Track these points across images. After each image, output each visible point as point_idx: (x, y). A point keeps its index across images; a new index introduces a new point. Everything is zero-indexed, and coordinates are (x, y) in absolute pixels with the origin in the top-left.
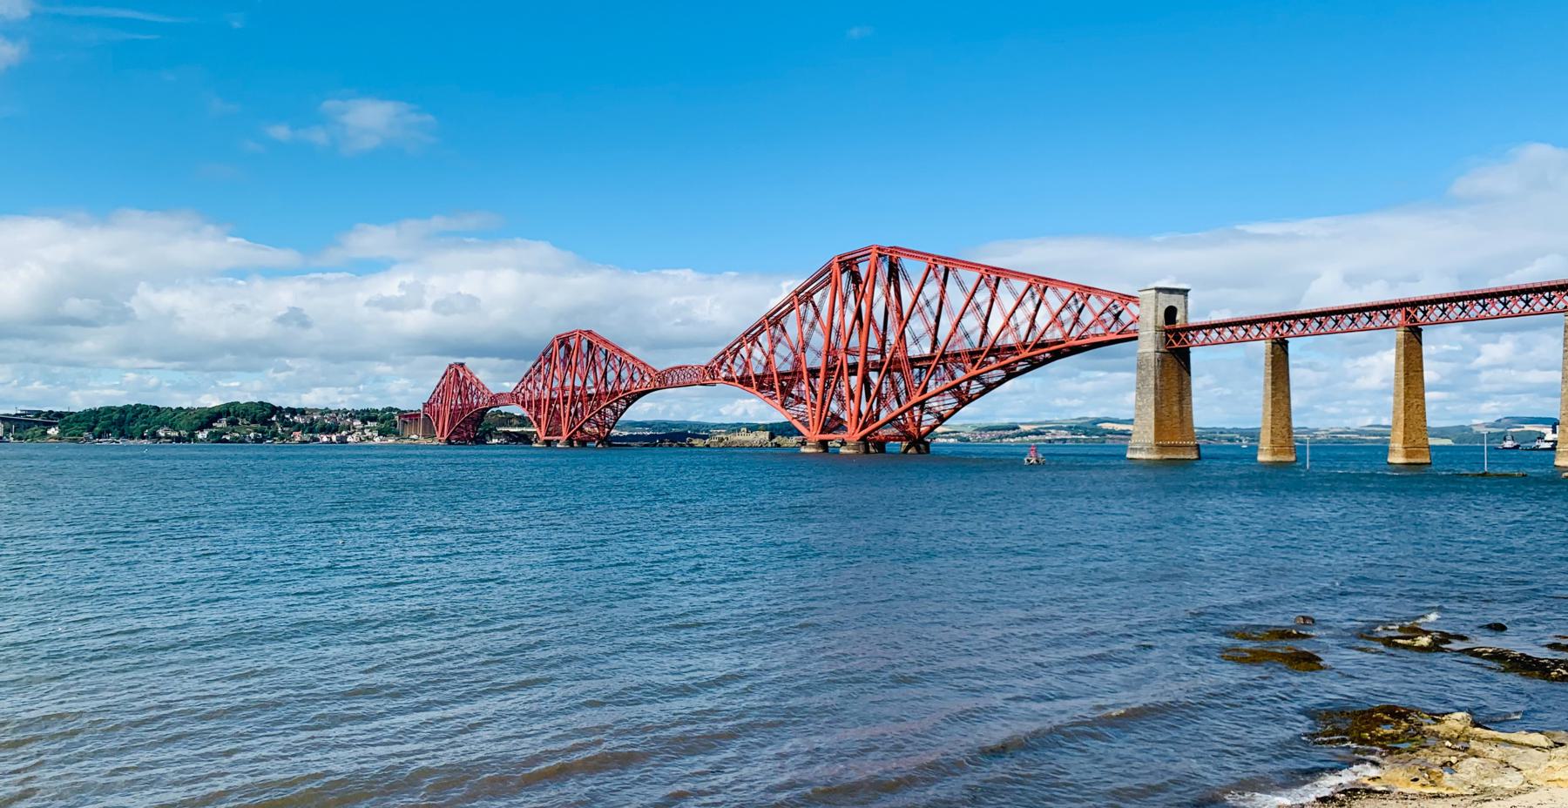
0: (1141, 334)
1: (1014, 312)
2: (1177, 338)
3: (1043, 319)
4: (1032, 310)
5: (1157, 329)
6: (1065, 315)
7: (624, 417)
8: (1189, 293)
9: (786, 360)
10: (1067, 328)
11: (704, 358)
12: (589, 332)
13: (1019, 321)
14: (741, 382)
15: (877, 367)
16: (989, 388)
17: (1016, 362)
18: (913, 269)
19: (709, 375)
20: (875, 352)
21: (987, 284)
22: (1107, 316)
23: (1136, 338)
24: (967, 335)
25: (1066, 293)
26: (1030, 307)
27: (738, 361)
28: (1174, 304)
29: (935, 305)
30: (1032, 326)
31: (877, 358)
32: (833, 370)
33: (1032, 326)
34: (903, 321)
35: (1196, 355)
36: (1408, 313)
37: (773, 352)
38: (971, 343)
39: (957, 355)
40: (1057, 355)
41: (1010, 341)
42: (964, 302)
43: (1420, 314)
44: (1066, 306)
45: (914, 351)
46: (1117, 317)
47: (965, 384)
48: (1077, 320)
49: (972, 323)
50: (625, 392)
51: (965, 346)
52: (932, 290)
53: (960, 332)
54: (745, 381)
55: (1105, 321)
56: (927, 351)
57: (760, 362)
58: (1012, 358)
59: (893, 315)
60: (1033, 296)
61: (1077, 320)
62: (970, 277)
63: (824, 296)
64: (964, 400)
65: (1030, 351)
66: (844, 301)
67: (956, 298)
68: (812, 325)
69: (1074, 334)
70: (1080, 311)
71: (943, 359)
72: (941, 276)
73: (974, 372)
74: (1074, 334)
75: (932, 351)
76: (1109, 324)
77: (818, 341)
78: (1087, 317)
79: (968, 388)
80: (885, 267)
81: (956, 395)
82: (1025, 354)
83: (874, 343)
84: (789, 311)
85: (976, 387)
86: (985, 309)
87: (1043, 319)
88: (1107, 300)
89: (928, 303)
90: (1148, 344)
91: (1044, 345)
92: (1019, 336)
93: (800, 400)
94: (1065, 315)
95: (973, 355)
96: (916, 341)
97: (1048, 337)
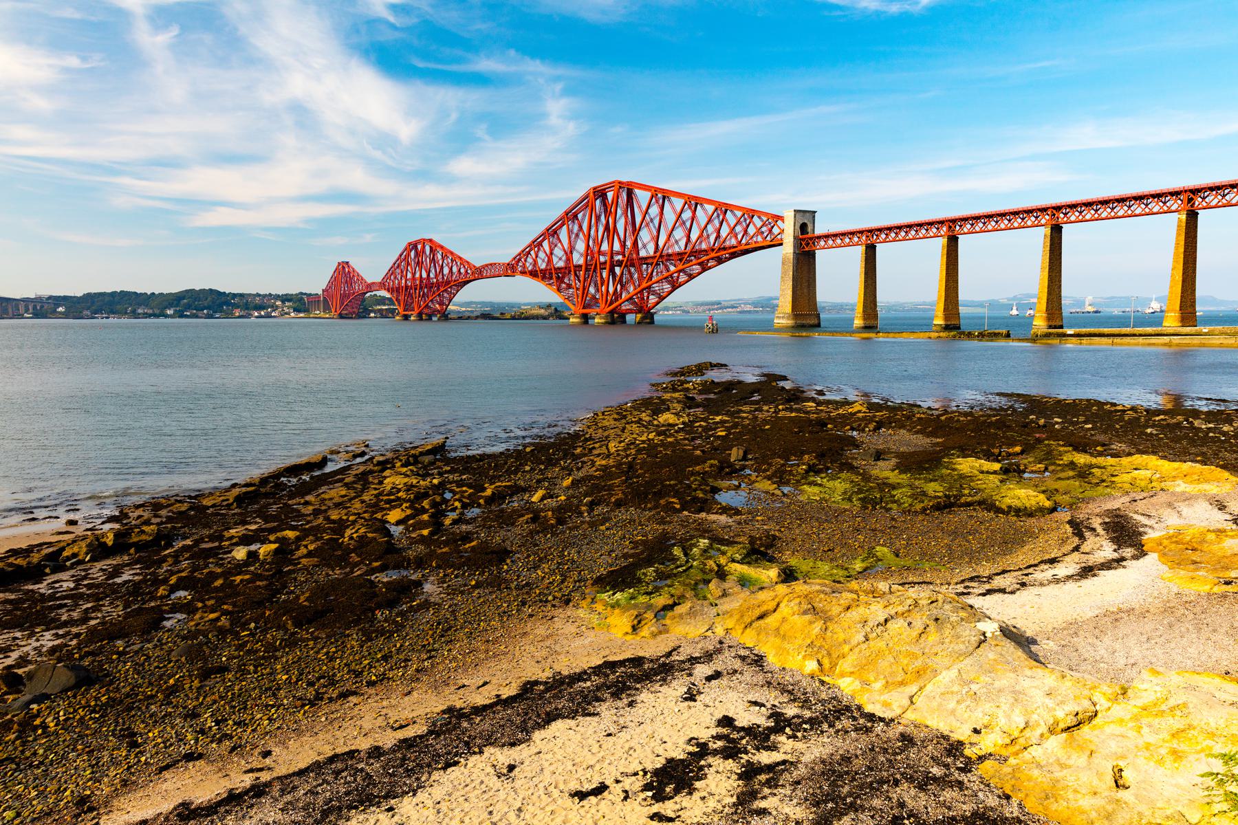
0: (785, 241)
2: (808, 244)
3: (725, 231)
4: (718, 225)
5: (795, 238)
6: (738, 229)
9: (560, 259)
10: (739, 237)
12: (431, 240)
15: (619, 263)
16: (691, 277)
17: (708, 261)
18: (642, 197)
19: (510, 269)
20: (618, 253)
22: (764, 229)
23: (781, 244)
24: (677, 242)
25: (739, 214)
26: (717, 223)
27: (530, 260)
29: (656, 222)
30: (718, 236)
31: (620, 257)
32: (591, 267)
33: (718, 236)
34: (636, 231)
35: (819, 254)
36: (950, 227)
37: (551, 254)
38: (680, 247)
39: (669, 255)
40: (734, 256)
41: (704, 246)
42: (674, 219)
43: (958, 228)
44: (738, 222)
45: (643, 253)
46: (770, 231)
47: (676, 275)
48: (746, 232)
49: (679, 234)
51: (677, 249)
52: (654, 210)
53: (672, 240)
54: (534, 274)
55: (763, 233)
56: (652, 253)
57: (543, 261)
58: (705, 258)
59: (630, 228)
60: (718, 216)
61: (746, 232)
63: (584, 215)
64: (675, 286)
66: (598, 218)
67: (670, 216)
68: (577, 235)
69: (744, 241)
70: (748, 226)
71: (661, 257)
73: (681, 267)
74: (744, 241)
75: (655, 252)
77: (580, 246)
78: (752, 230)
79: (678, 277)
80: (624, 195)
81: (669, 282)
82: (713, 255)
83: (617, 247)
84: (561, 226)
85: (683, 278)
86: (688, 224)
87: (725, 231)
88: (765, 219)
89: (652, 220)
90: (788, 248)
91: (725, 249)
92: (709, 243)
93: (569, 286)
94: (738, 229)
95: (680, 256)
96: (644, 246)
97: (727, 244)
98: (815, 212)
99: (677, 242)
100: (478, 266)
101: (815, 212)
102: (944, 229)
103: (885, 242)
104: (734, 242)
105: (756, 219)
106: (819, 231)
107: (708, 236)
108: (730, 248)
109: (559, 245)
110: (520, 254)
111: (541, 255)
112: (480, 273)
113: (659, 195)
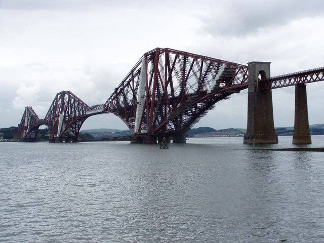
7: (81, 129)
12: (69, 93)
18: (172, 56)
19: (106, 110)
21: (198, 63)
28: (263, 69)
29: (180, 74)
51: (191, 91)
53: (188, 86)
54: (114, 111)
55: (239, 79)
62: (191, 59)
76: (241, 79)
86: (198, 74)
103: (309, 82)
106: (274, 74)
107: (208, 82)
109: (131, 92)
110: (110, 99)
111: (122, 99)
113: (181, 56)
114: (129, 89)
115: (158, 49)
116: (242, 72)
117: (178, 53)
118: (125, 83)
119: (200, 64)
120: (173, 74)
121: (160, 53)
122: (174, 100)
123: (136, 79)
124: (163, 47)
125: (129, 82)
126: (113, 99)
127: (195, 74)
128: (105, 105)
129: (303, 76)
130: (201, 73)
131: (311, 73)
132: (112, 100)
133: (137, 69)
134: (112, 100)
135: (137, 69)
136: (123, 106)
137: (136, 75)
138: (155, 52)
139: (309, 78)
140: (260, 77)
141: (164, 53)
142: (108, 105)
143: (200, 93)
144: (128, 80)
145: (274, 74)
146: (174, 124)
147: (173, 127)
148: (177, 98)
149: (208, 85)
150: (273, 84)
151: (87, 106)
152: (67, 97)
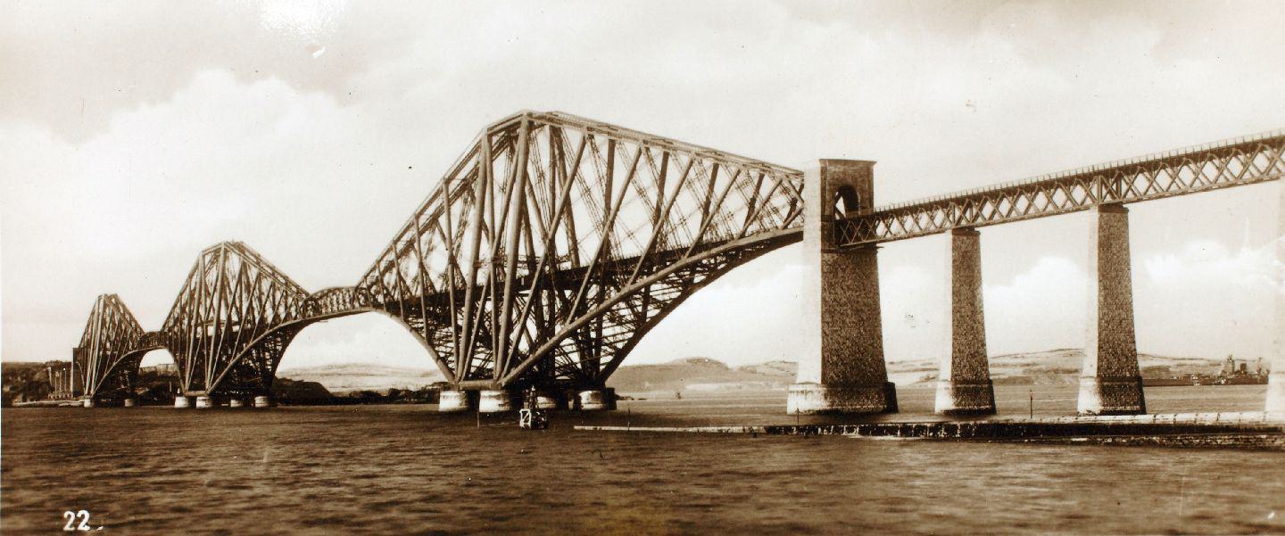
1: (674, 200)
8: (876, 170)
11: (350, 275)
12: (240, 248)
13: (686, 212)
14: (388, 310)
16: (666, 308)
18: (573, 138)
21: (650, 159)
29: (598, 194)
43: (1124, 187)
50: (272, 326)
53: (619, 231)
55: (776, 210)
64: (642, 326)
65: (690, 256)
71: (609, 269)
72: (604, 152)
76: (785, 212)
78: (757, 205)
82: (685, 260)
85: (652, 312)
86: (653, 195)
95: (635, 260)
98: (873, 163)
99: (630, 235)
100: (311, 291)
101: (873, 163)
102: (1095, 191)
104: (722, 232)
105: (768, 184)
106: (881, 202)
107: (683, 221)
108: (716, 245)
110: (373, 269)
112: (314, 309)
114: (437, 238)
115: (530, 115)
116: (785, 191)
117: (589, 129)
118: (423, 220)
119: (659, 162)
120: (575, 193)
121: (531, 127)
122: (574, 278)
123: (457, 207)
124: (540, 106)
125: (434, 220)
126: (389, 268)
127: (641, 192)
128: (357, 289)
129: (970, 206)
130: (661, 193)
131: (996, 196)
132: (383, 274)
133: (462, 175)
134: (383, 274)
135: (462, 175)
136: (417, 292)
137: (457, 195)
138: (518, 124)
139: (988, 209)
140: (840, 205)
141: (547, 128)
142: (369, 288)
143: (657, 257)
144: (431, 210)
145: (881, 202)
146: (580, 350)
147: (575, 357)
148: (585, 269)
149: (680, 230)
150: (881, 229)
151: (300, 291)
152: (234, 263)
